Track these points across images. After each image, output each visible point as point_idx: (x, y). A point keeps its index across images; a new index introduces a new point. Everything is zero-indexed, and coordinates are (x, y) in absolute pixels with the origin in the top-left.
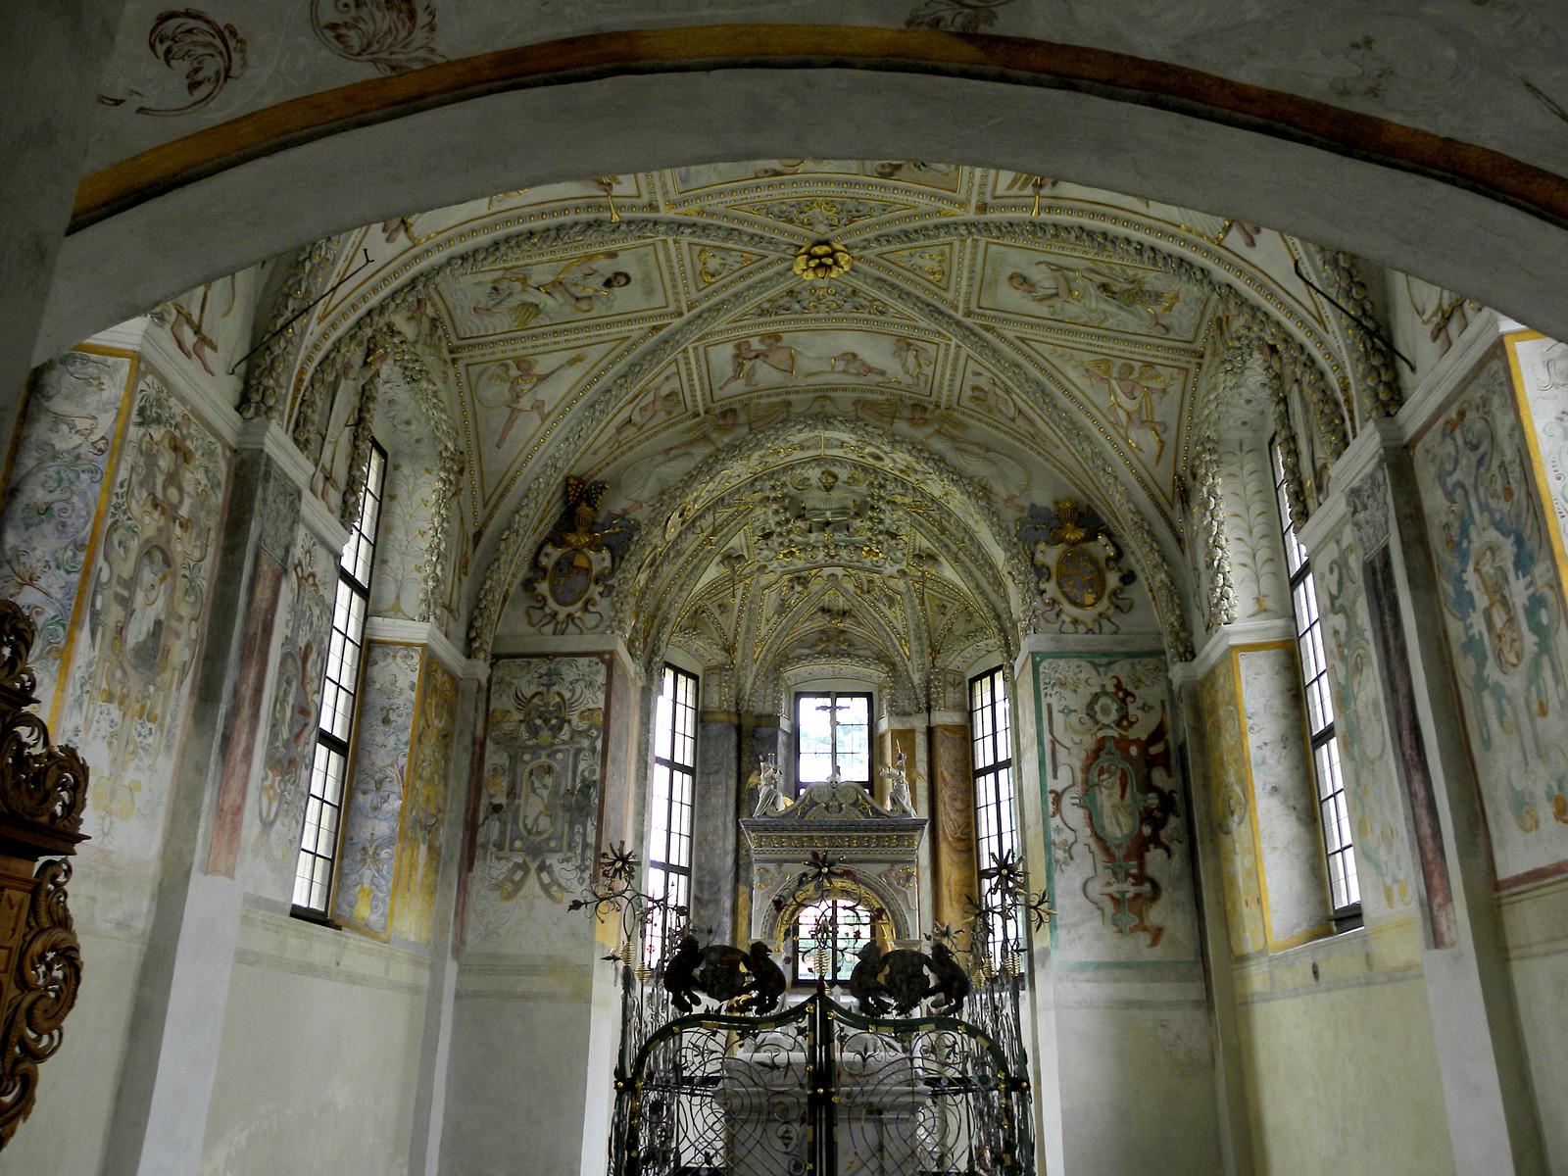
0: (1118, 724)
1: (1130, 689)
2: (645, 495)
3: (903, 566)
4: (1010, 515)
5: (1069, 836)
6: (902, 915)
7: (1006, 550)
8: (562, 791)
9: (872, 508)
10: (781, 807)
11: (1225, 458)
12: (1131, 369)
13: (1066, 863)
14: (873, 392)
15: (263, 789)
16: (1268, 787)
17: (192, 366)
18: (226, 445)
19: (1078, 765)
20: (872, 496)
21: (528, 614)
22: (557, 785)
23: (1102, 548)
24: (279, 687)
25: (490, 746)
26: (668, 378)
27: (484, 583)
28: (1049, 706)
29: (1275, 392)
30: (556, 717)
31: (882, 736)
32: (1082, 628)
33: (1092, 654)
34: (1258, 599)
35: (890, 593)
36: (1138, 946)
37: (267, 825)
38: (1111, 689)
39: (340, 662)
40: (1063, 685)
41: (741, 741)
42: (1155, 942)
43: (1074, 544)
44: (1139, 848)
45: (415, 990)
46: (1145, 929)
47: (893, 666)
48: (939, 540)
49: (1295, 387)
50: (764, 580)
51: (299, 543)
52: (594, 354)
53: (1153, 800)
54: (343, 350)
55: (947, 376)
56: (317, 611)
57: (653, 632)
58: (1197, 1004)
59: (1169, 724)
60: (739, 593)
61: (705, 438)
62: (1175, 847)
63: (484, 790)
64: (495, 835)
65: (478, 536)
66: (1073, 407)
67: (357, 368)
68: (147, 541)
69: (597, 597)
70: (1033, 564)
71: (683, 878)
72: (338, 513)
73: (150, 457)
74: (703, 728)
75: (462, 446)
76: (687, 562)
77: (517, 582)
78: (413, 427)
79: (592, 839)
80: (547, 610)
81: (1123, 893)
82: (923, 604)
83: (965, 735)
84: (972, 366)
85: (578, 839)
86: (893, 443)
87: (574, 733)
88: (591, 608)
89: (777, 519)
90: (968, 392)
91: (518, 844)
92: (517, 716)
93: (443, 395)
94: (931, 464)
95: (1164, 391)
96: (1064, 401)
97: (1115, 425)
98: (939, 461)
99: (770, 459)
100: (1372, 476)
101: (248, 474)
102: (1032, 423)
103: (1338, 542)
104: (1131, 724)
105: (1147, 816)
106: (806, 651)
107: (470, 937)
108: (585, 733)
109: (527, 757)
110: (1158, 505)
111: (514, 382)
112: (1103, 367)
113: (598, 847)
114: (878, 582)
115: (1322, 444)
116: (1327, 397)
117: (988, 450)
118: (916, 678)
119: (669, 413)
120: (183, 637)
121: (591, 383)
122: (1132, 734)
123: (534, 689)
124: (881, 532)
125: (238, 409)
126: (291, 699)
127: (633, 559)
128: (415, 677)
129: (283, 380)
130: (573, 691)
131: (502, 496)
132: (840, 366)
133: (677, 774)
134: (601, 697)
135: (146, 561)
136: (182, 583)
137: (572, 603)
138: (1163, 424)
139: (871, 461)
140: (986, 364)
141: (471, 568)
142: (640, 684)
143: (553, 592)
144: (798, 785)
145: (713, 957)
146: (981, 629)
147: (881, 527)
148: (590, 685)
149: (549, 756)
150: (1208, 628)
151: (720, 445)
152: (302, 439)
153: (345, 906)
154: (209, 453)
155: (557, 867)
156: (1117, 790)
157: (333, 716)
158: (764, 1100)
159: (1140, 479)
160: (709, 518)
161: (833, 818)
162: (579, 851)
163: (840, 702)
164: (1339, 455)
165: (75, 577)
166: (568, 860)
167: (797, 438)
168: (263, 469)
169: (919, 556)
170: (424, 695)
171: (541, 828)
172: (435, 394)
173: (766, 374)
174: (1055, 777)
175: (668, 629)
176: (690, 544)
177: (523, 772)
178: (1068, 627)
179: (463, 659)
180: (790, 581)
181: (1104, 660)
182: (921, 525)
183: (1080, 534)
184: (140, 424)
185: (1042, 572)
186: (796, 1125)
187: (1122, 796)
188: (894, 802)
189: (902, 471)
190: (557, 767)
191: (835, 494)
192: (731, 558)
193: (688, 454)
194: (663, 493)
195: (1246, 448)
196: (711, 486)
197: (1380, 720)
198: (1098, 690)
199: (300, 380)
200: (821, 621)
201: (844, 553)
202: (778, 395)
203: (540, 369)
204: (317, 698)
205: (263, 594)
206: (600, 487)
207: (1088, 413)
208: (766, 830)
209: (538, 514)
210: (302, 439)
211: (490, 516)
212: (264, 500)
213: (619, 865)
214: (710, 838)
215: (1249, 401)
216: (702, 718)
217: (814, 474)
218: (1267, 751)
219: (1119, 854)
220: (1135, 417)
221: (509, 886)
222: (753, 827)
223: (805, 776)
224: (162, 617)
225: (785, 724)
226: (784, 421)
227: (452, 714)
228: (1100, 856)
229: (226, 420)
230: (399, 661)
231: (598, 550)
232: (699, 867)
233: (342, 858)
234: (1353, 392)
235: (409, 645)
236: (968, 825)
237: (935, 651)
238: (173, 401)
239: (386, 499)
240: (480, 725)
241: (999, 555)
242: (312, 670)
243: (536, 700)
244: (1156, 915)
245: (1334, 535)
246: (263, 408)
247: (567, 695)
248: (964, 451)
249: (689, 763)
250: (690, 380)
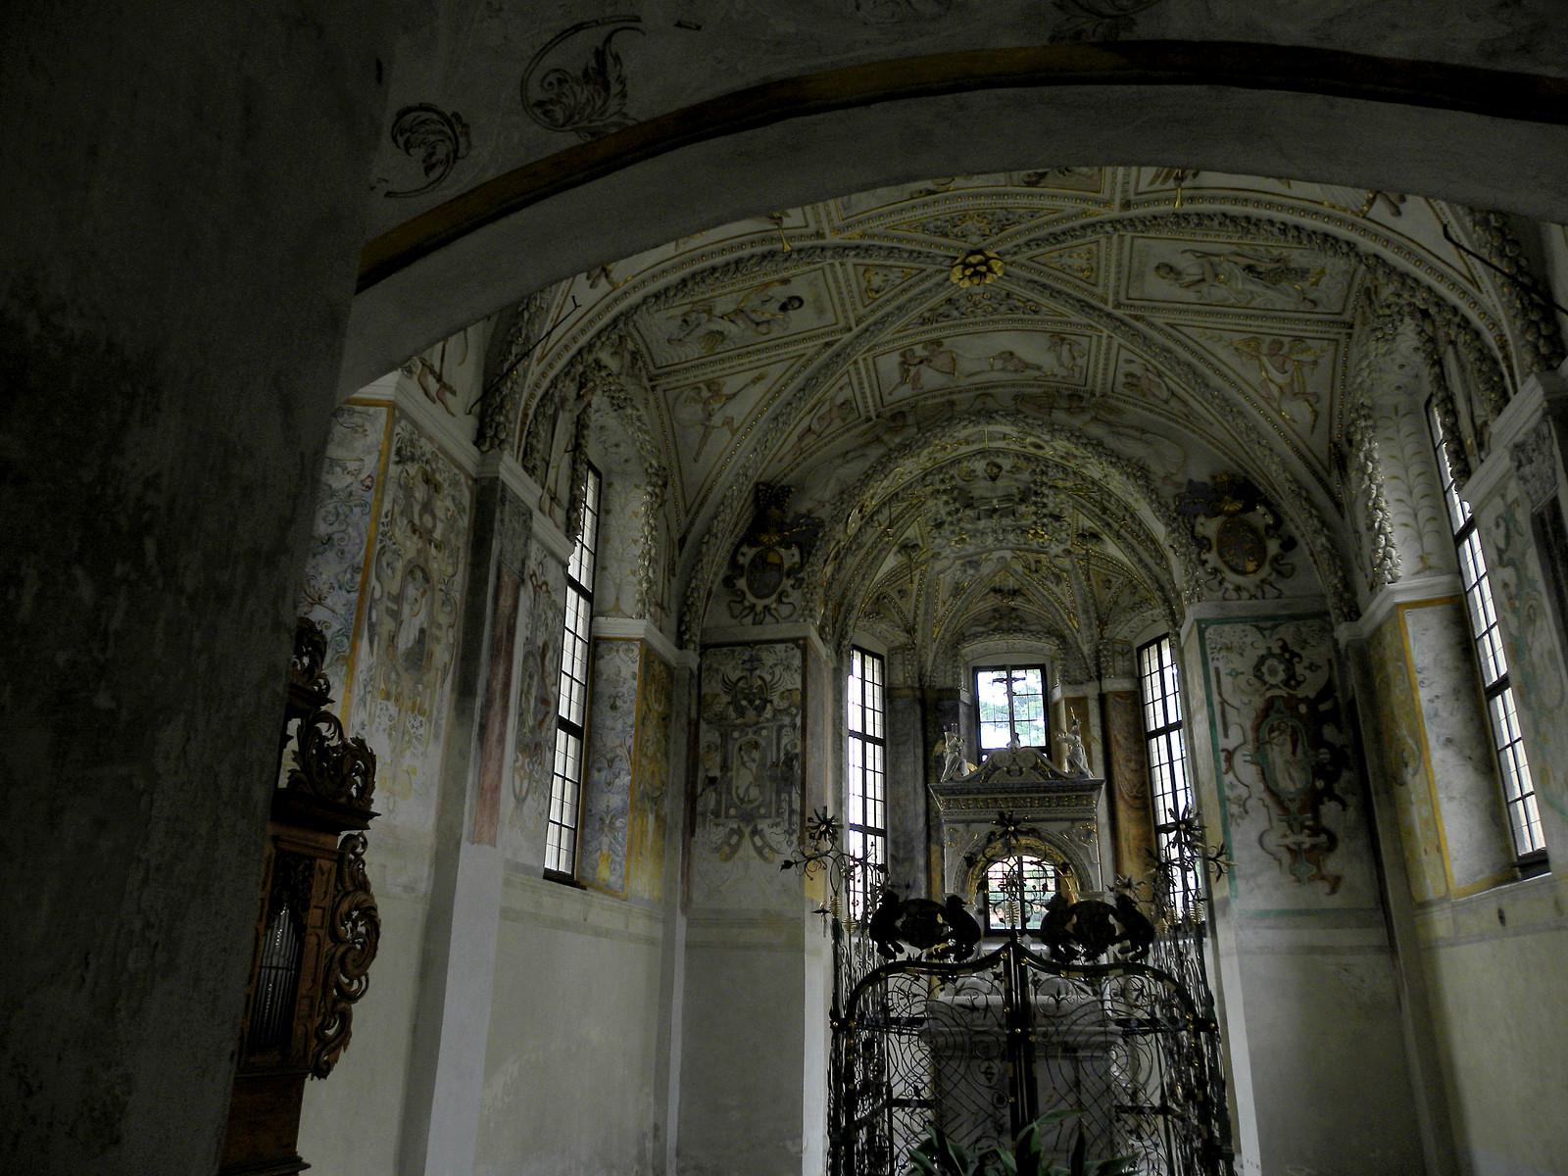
0: (1286, 683)
1: (1296, 649)
2: (827, 495)
3: (1068, 545)
4: (1168, 492)
5: (1243, 791)
6: (1085, 869)
7: (1167, 525)
8: (769, 764)
9: (1036, 494)
10: (966, 773)
11: (1379, 423)
12: (1282, 344)
13: (1243, 818)
14: (1030, 386)
15: (515, 770)
16: (1442, 739)
17: (437, 409)
18: (468, 476)
19: (1248, 724)
20: (1035, 482)
21: (729, 607)
22: (764, 757)
23: (1260, 517)
24: (523, 682)
25: (703, 726)
26: (841, 389)
27: (690, 582)
28: (1217, 670)
29: (1429, 355)
30: (760, 698)
31: (1057, 704)
32: (1245, 595)
33: (1257, 619)
34: (1422, 558)
35: (1057, 571)
36: (1318, 895)
37: (520, 801)
38: (1277, 650)
39: (572, 659)
40: (1229, 649)
41: (926, 713)
42: (1333, 891)
43: (1232, 515)
44: (1313, 800)
45: (651, 941)
46: (1323, 878)
47: (1062, 639)
48: (1101, 519)
49: (1450, 349)
50: (938, 565)
51: (533, 554)
52: (775, 371)
53: (1324, 754)
54: (560, 386)
55: (1101, 366)
56: (550, 614)
57: (840, 618)
58: (1380, 949)
59: (1337, 682)
60: (916, 580)
61: (878, 439)
62: (1351, 800)
63: (701, 767)
64: (712, 804)
65: (682, 541)
66: (1226, 386)
67: (572, 401)
68: (410, 561)
69: (789, 589)
70: (1193, 537)
71: (879, 839)
72: (563, 528)
73: (407, 489)
74: (891, 702)
75: (664, 463)
77: (719, 579)
78: (622, 449)
79: (797, 806)
80: (747, 604)
81: (1299, 845)
82: (1089, 579)
83: (1136, 701)
84: (1124, 354)
85: (785, 805)
86: (1052, 432)
87: (776, 712)
88: (784, 600)
90: (1121, 379)
91: (732, 811)
92: (726, 699)
93: (645, 419)
94: (1090, 449)
95: (1315, 363)
96: (1216, 381)
97: (1268, 399)
98: (1097, 446)
99: (938, 455)
100: (1536, 430)
101: (488, 497)
102: (1185, 403)
103: (1503, 496)
104: (1299, 683)
105: (1318, 771)
106: (981, 629)
107: (696, 896)
108: (786, 711)
109: (736, 735)
110: (1314, 473)
111: (706, 403)
112: (1253, 344)
113: (803, 814)
115: (1481, 402)
116: (1484, 355)
117: (1143, 431)
118: (1086, 649)
119: (844, 420)
120: (444, 641)
121: (773, 398)
122: (1300, 693)
123: (738, 674)
124: (1045, 516)
125: (476, 443)
126: (534, 692)
128: (636, 667)
129: (511, 416)
130: (773, 674)
131: (701, 504)
132: (999, 364)
133: (870, 746)
134: (798, 679)
135: (410, 579)
136: (439, 596)
137: (768, 596)
138: (1315, 394)
139: (1032, 450)
140: (1137, 351)
141: (678, 571)
142: (831, 666)
143: (750, 587)
144: (981, 752)
145: (913, 909)
146: (1145, 601)
147: (1045, 511)
148: (788, 668)
149: (755, 733)
150: (1372, 588)
151: (892, 445)
152: (530, 466)
153: (588, 869)
154: (455, 484)
155: (768, 831)
156: (1289, 747)
157: (569, 706)
158: (966, 1039)
159: (1296, 450)
160: (886, 512)
161: (1015, 781)
162: (786, 816)
163: (1016, 674)
164: (1500, 411)
165: (354, 596)
166: (777, 825)
167: (963, 434)
168: (499, 495)
169: (1083, 536)
170: (645, 684)
171: (752, 797)
172: (639, 419)
173: (930, 378)
174: (1226, 736)
175: (855, 612)
176: (870, 536)
177: (733, 747)
178: (1233, 595)
179: (676, 650)
180: (963, 565)
181: (1269, 624)
182: (1083, 506)
183: (1239, 505)
184: (398, 463)
185: (1203, 543)
186: (997, 1062)
187: (1294, 753)
188: (1072, 764)
190: (763, 743)
191: (1000, 483)
192: (907, 548)
193: (863, 455)
194: (843, 492)
195: (1402, 412)
196: (885, 483)
197: (1557, 669)
198: (1264, 652)
199: (526, 415)
200: (993, 601)
201: (1011, 537)
202: (942, 395)
203: (726, 390)
204: (555, 689)
205: (505, 601)
206: (786, 491)
207: (1240, 390)
208: (953, 793)
209: (733, 518)
210: (530, 466)
211: (692, 523)
212: (502, 520)
213: (823, 828)
214: (902, 802)
215: (1402, 366)
216: (889, 694)
217: (980, 466)
218: (1439, 704)
219: (1294, 807)
220: (1287, 390)
221: (727, 849)
222: (942, 791)
223: (986, 744)
224: (425, 626)
225: (965, 697)
226: (949, 419)
227: (669, 699)
228: (1275, 811)
229: (466, 454)
230: (621, 653)
231: (788, 547)
232: (894, 829)
233: (583, 827)
234: (1512, 348)
235: (629, 640)
236: (1143, 784)
237: (1103, 623)
238: (423, 441)
239: (602, 514)
240: (694, 708)
241: (1159, 530)
242: (550, 667)
243: (741, 684)
244: (1333, 864)
245: (1499, 490)
246: (497, 442)
247: (768, 678)
248: (1119, 434)
249: (878, 735)
250: (862, 388)
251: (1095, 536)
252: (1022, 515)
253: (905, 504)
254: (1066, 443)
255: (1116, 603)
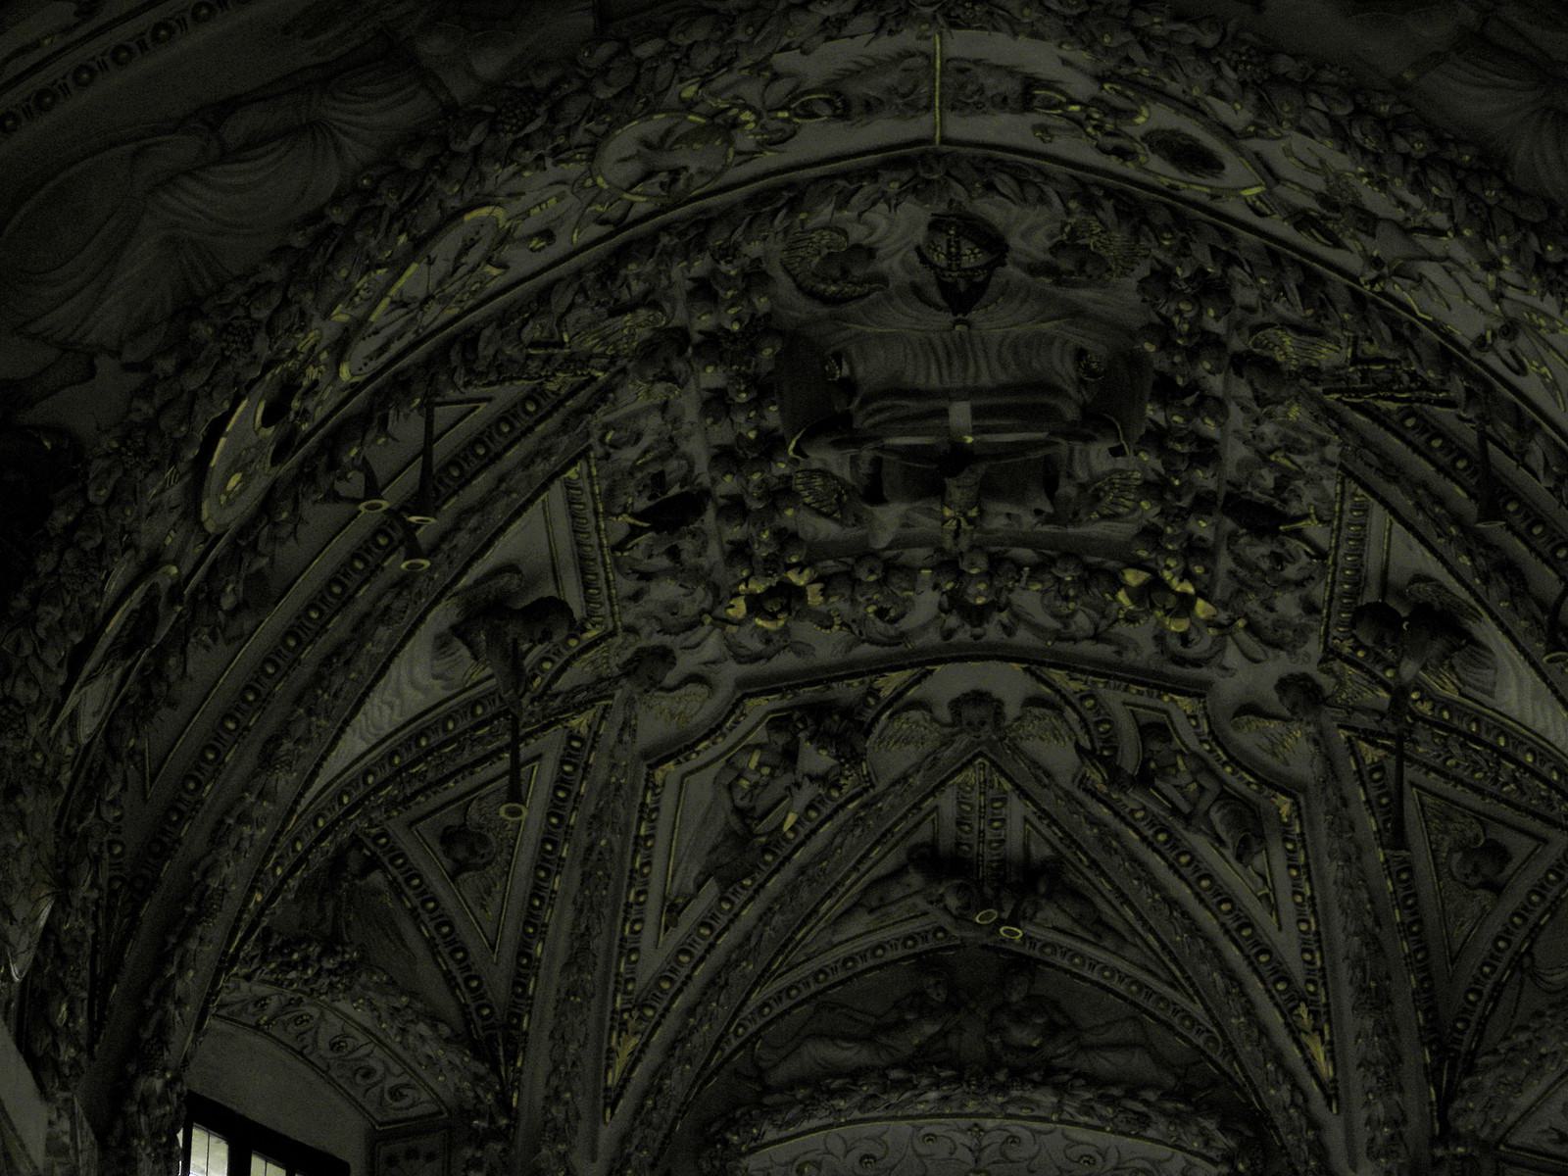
3: (1308, 658)
9: (1166, 391)
20: (1163, 332)
35: (1242, 783)
48: (1474, 541)
76: (298, 631)
82: (1395, 836)
86: (1263, 90)
89: (722, 434)
99: (693, 159)
106: (849, 1055)
114: (1188, 735)
124: (1204, 504)
127: (51, 614)
139: (1160, 170)
147: (1204, 478)
151: (460, 89)
160: (407, 428)
167: (819, 63)
169: (1379, 617)
175: (215, 929)
176: (319, 543)
180: (778, 722)
182: (1392, 470)
189: (1302, 220)
191: (994, 322)
194: (189, 308)
196: (414, 279)
200: (919, 915)
201: (1029, 598)
217: (895, 228)
237: (1453, 1062)
251: (1440, 626)
252: (1092, 494)
253: (506, 393)
254: (1326, 149)
255: (1523, 965)
